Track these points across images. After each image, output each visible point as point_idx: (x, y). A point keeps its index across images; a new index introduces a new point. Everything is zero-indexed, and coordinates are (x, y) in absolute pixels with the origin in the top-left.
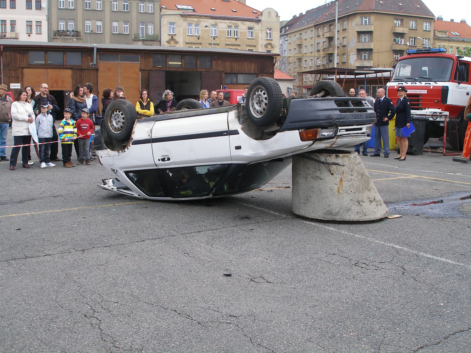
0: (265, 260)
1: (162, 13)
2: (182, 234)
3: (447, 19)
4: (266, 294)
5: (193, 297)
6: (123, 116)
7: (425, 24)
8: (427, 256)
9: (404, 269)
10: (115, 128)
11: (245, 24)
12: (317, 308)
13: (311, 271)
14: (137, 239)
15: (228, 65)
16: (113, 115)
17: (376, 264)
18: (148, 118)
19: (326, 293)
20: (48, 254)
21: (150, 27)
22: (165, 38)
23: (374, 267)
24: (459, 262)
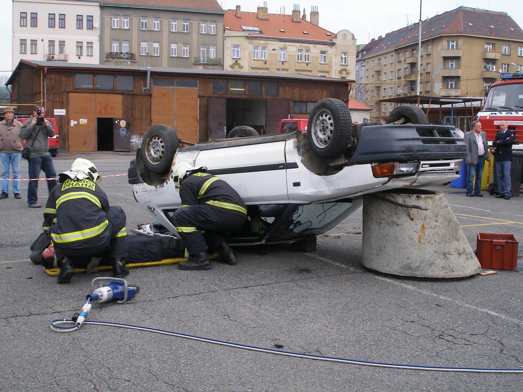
0: (324, 328)
1: (225, 35)
2: (224, 290)
4: (322, 375)
6: (163, 144)
7: (520, 49)
9: (502, 344)
10: (153, 158)
13: (383, 345)
14: (169, 294)
15: (296, 93)
16: (151, 143)
17: (466, 336)
18: (191, 147)
19: (400, 377)
20: (57, 311)
21: (212, 50)
22: (228, 62)
23: (463, 342)
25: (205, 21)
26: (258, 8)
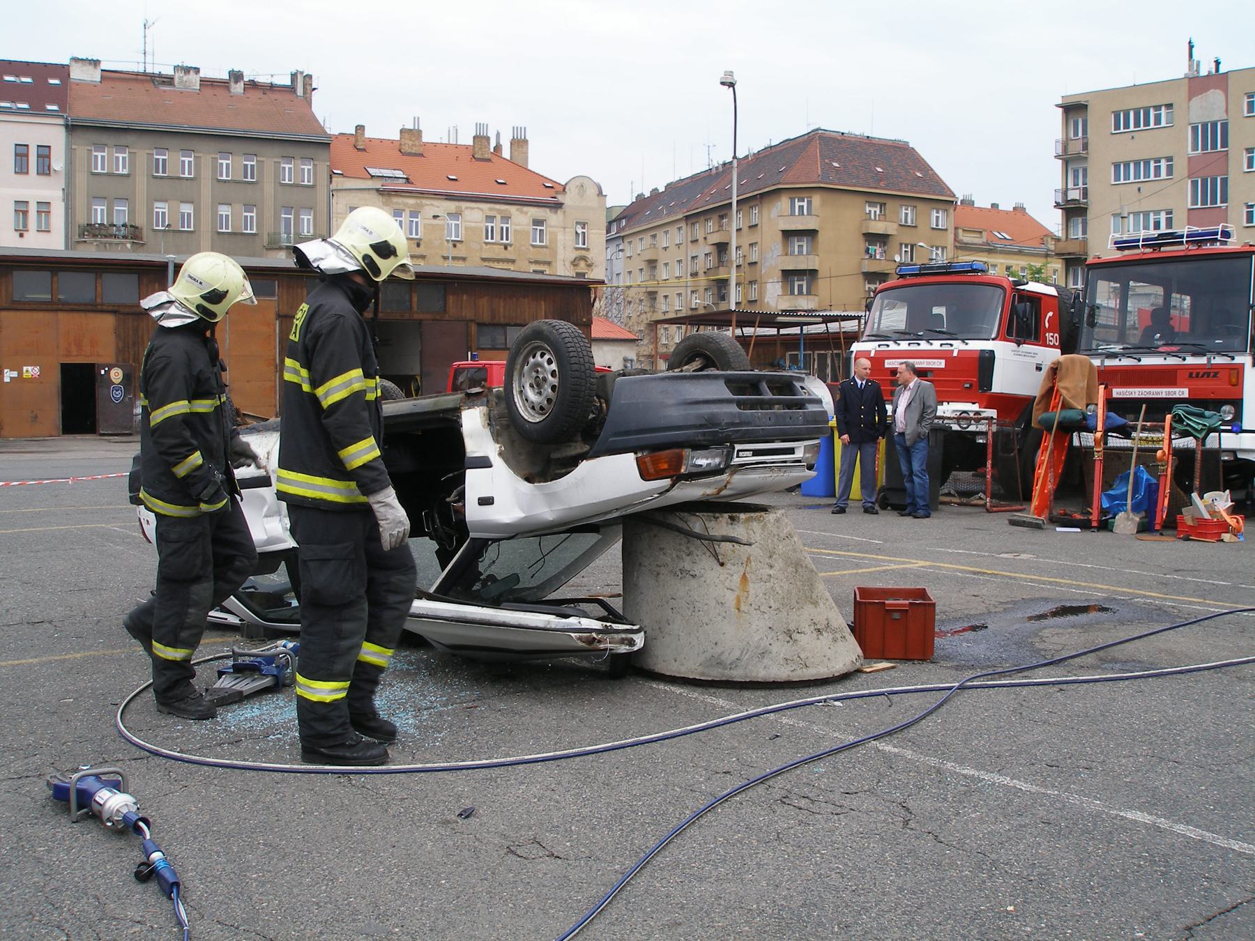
0: (548, 793)
1: (333, 186)
3: (982, 202)
4: (545, 890)
5: (349, 904)
7: (934, 214)
8: (965, 772)
11: (526, 213)
12: (680, 930)
15: (484, 307)
17: (836, 797)
23: (831, 808)
24: (1046, 787)
25: (289, 158)
26: (402, 131)
